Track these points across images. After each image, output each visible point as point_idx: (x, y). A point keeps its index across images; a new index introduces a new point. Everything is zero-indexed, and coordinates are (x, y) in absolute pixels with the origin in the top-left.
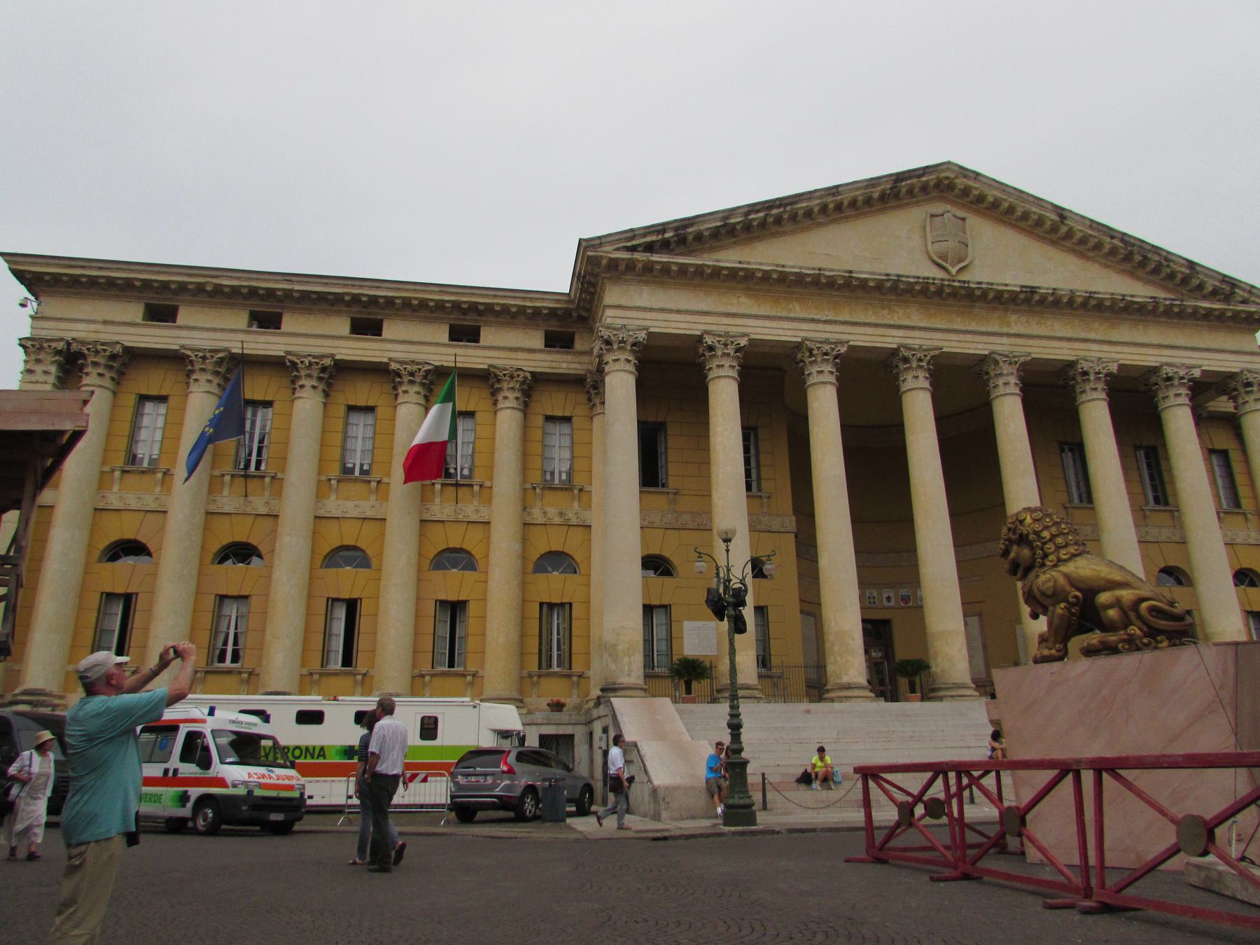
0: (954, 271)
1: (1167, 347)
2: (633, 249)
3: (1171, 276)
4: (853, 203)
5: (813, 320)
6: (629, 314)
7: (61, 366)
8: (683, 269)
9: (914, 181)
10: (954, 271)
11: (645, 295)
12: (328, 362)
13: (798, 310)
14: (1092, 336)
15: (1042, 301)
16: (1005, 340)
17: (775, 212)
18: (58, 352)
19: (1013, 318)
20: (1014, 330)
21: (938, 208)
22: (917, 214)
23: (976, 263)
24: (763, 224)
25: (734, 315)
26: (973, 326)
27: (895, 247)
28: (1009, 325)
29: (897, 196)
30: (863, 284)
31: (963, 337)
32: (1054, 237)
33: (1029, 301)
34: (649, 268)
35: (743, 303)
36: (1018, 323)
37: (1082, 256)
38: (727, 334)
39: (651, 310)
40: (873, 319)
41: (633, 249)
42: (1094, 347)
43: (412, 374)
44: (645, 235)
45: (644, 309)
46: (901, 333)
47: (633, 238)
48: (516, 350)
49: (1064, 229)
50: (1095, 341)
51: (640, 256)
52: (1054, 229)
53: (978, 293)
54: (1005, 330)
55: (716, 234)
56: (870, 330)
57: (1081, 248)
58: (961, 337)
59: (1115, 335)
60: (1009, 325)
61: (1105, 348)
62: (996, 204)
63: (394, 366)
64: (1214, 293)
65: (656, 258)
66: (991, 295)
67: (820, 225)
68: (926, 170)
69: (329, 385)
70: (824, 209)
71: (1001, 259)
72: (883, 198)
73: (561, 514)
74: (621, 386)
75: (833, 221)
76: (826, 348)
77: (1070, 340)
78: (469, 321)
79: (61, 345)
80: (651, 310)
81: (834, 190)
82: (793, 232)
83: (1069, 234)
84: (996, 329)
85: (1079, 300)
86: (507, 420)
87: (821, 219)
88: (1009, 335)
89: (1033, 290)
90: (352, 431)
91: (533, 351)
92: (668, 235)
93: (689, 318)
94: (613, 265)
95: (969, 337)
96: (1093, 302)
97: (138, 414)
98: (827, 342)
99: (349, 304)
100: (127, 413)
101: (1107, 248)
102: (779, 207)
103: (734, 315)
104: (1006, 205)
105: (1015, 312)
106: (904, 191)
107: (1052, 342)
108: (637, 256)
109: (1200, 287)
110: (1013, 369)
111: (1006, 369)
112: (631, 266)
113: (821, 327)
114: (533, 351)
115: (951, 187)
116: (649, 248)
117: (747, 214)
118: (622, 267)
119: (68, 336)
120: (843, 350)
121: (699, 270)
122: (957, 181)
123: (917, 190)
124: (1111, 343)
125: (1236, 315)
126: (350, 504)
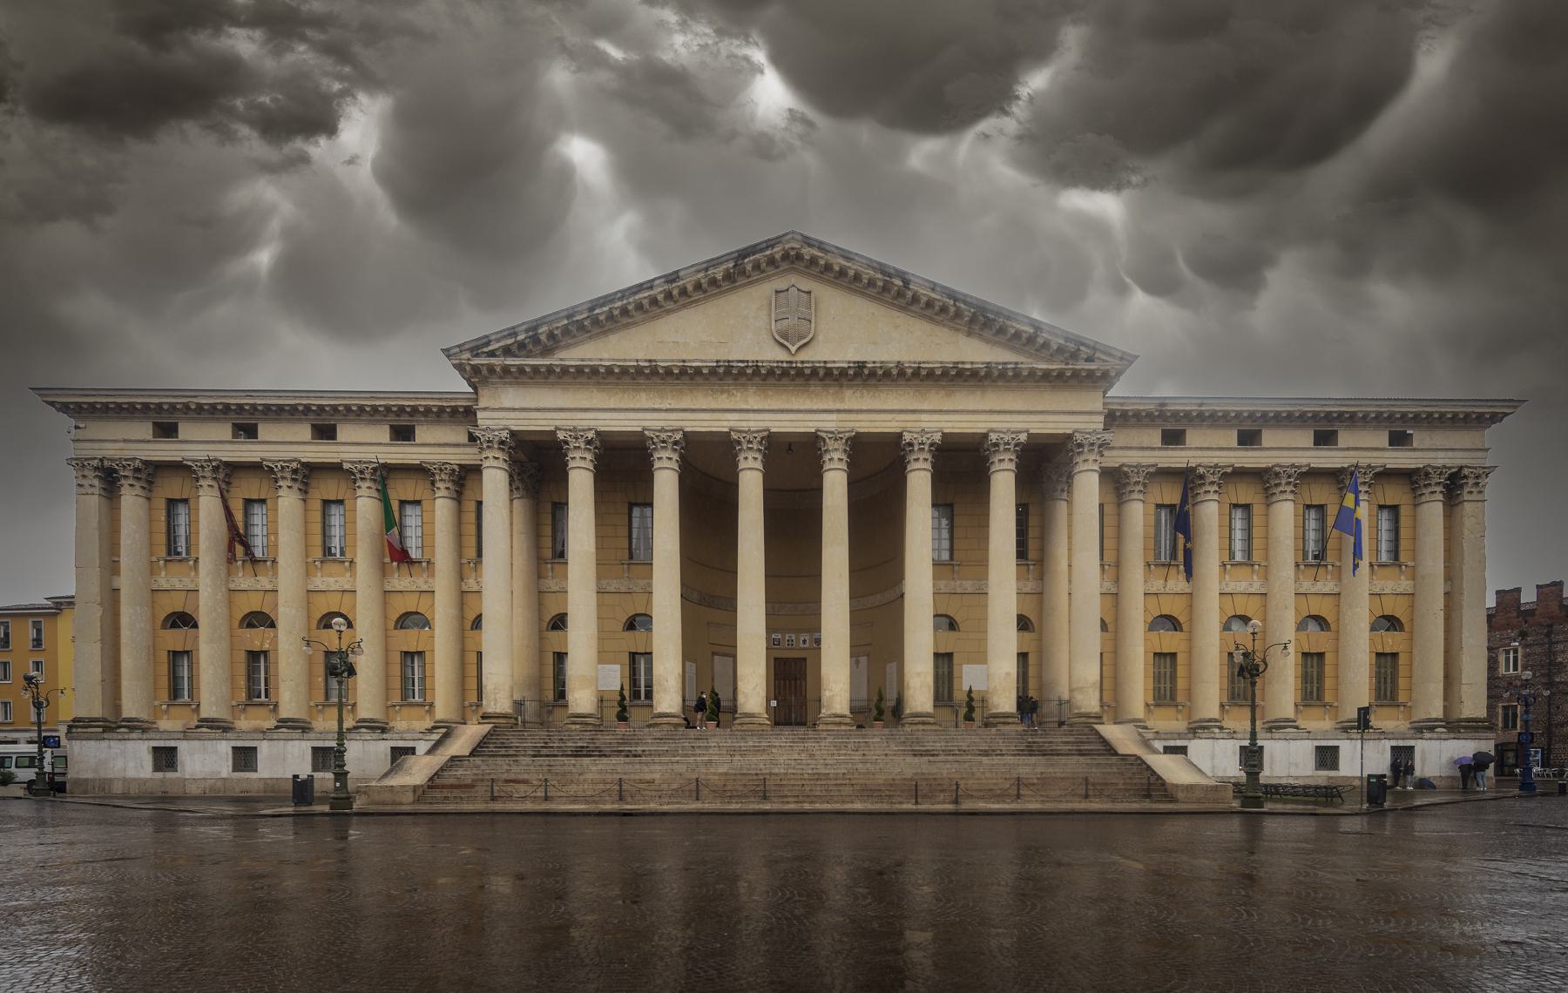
0: (793, 349)
1: (999, 412)
2: (492, 354)
3: (1017, 335)
4: (698, 286)
5: (655, 410)
8: (536, 369)
10: (793, 349)
13: (643, 400)
14: (925, 407)
15: (873, 373)
16: (834, 416)
19: (848, 393)
21: (780, 283)
22: (766, 289)
23: (820, 337)
24: (610, 317)
26: (808, 405)
29: (743, 273)
30: (698, 371)
31: (794, 414)
32: (902, 301)
33: (862, 376)
34: (506, 370)
36: (853, 399)
37: (931, 320)
38: (575, 429)
39: (514, 409)
40: (714, 405)
42: (924, 417)
44: (498, 340)
47: (488, 344)
49: (909, 294)
52: (900, 294)
56: (708, 414)
57: (929, 312)
60: (842, 400)
61: (936, 417)
62: (842, 273)
64: (1060, 350)
65: (510, 361)
66: (822, 373)
67: (669, 312)
71: (849, 331)
72: (728, 277)
75: (684, 306)
76: (663, 436)
80: (514, 409)
82: (644, 321)
83: (915, 299)
85: (909, 371)
87: (670, 305)
88: (839, 411)
89: (861, 365)
95: (801, 416)
96: (924, 373)
98: (662, 430)
101: (952, 309)
102: (621, 299)
104: (851, 273)
105: (849, 387)
106: (749, 267)
107: (878, 413)
108: (493, 361)
109: (1046, 345)
110: (840, 445)
111: (831, 444)
115: (799, 257)
116: (507, 351)
117: (591, 309)
118: (485, 372)
121: (550, 370)
122: (803, 251)
123: (763, 265)
124: (941, 412)
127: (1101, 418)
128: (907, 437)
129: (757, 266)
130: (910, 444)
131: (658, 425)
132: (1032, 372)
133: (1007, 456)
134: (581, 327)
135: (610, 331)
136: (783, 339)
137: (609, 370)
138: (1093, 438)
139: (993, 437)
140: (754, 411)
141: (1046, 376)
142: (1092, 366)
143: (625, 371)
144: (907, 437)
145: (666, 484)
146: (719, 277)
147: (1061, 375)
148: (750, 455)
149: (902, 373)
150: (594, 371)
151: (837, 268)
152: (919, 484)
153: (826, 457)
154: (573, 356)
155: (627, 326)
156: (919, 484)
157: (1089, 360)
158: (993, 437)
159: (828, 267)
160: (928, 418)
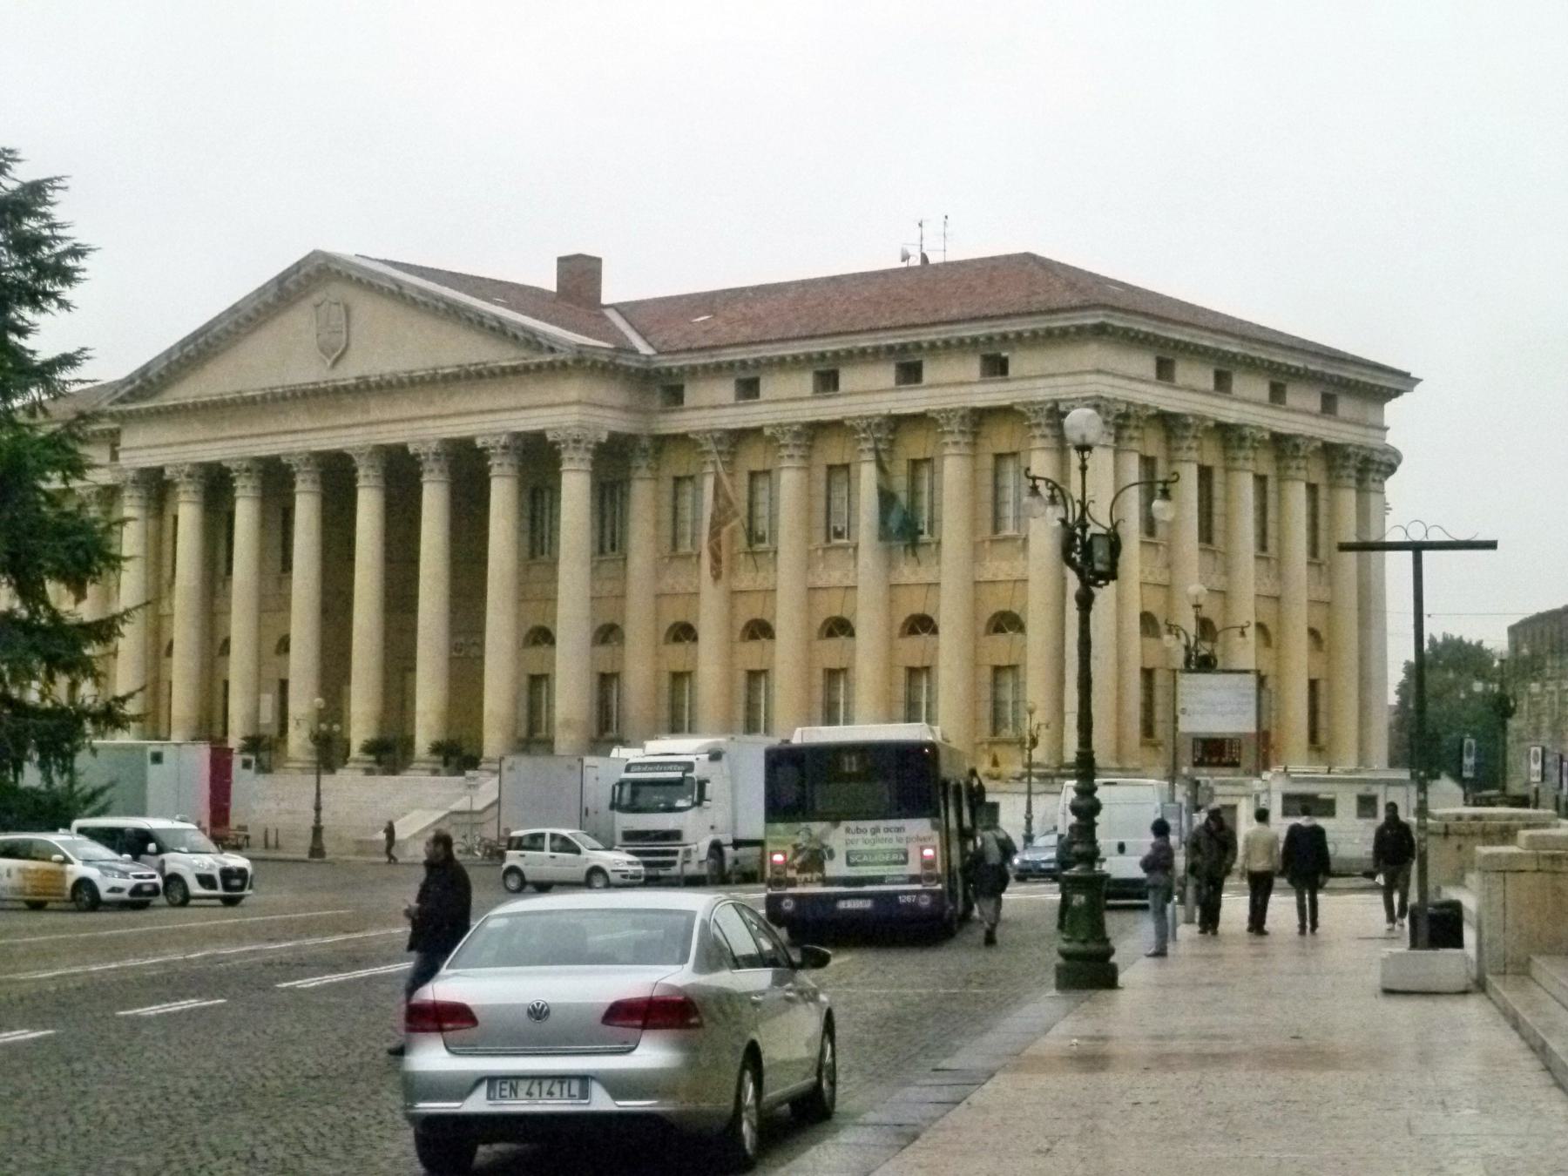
2: (122, 401)
9: (294, 277)
10: (329, 363)
16: (359, 431)
17: (201, 340)
19: (373, 403)
21: (316, 298)
24: (200, 352)
27: (284, 357)
28: (368, 412)
35: (197, 430)
42: (429, 423)
46: (289, 438)
51: (121, 407)
65: (132, 407)
68: (298, 266)
72: (279, 298)
81: (234, 309)
87: (243, 331)
113: (239, 442)
129: (298, 283)
143: (205, 405)
146: (271, 300)
154: (168, 399)
155: (216, 354)
159: (349, 277)
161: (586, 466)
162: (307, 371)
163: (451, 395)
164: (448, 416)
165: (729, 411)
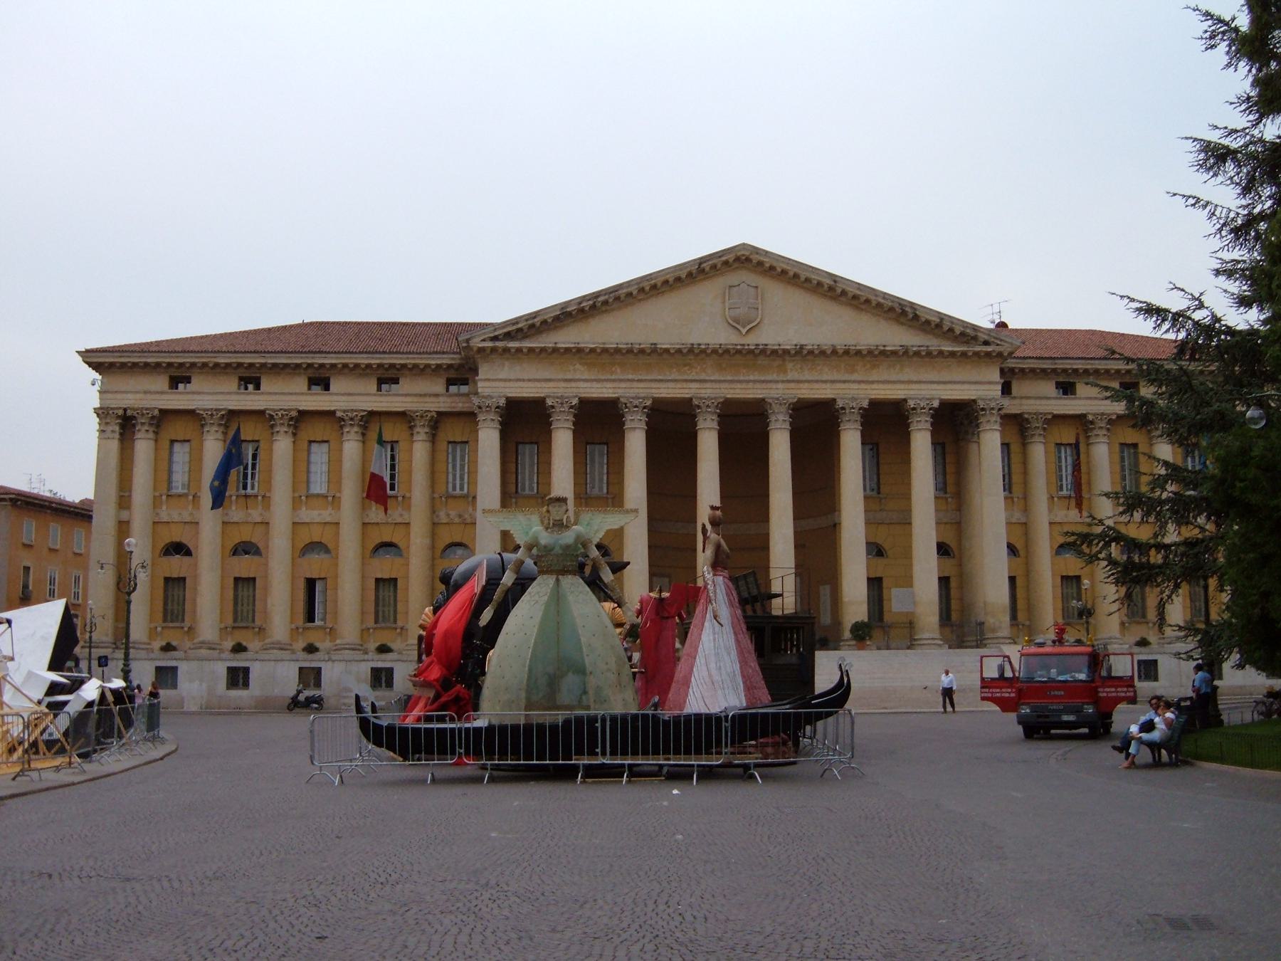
1: (916, 382)
2: (495, 339)
6: (494, 384)
7: (122, 426)
8: (531, 350)
10: (744, 331)
11: (506, 368)
12: (294, 414)
18: (118, 417)
19: (790, 365)
20: (789, 378)
24: (593, 307)
25: (570, 380)
28: (785, 372)
30: (667, 351)
31: (745, 388)
33: (802, 354)
34: (506, 350)
35: (579, 370)
41: (495, 339)
43: (352, 419)
45: (505, 380)
48: (425, 395)
50: (854, 382)
51: (499, 344)
53: (757, 352)
54: (782, 377)
55: (557, 318)
58: (744, 386)
59: (874, 376)
61: (863, 386)
63: (339, 414)
69: (296, 427)
70: (642, 290)
73: (460, 516)
74: (489, 438)
76: (636, 402)
77: (833, 382)
78: (391, 374)
79: (120, 412)
82: (620, 308)
84: (774, 377)
85: (841, 352)
86: (419, 451)
89: (802, 347)
90: (313, 458)
91: (437, 395)
92: (520, 326)
93: (538, 384)
94: (481, 350)
97: (171, 453)
99: (306, 369)
100: (165, 454)
103: (570, 380)
110: (784, 409)
111: (776, 408)
112: (494, 350)
114: (437, 395)
119: (124, 404)
120: (649, 403)
125: (976, 354)
126: (316, 512)
127: (1000, 387)
128: (840, 404)
130: (843, 408)
131: (632, 393)
132: (941, 353)
133: (923, 418)
134: (569, 314)
135: (592, 316)
136: (736, 324)
137: (592, 350)
138: (993, 405)
139: (911, 403)
140: (712, 381)
141: (952, 354)
142: (989, 349)
144: (840, 404)
145: (636, 445)
147: (964, 354)
148: (709, 417)
149: (834, 352)
150: (580, 351)
151: (779, 270)
152: (851, 443)
153: (773, 418)
154: (566, 337)
156: (851, 443)
157: (986, 343)
158: (911, 403)
160: (854, 390)
161: (928, 426)
162: (717, 335)
163: (874, 367)
164: (873, 382)
165: (1053, 402)
